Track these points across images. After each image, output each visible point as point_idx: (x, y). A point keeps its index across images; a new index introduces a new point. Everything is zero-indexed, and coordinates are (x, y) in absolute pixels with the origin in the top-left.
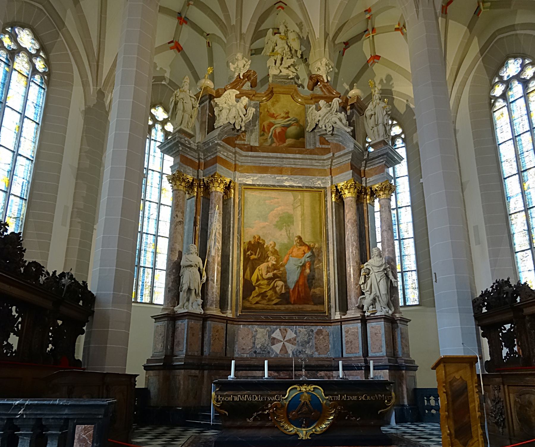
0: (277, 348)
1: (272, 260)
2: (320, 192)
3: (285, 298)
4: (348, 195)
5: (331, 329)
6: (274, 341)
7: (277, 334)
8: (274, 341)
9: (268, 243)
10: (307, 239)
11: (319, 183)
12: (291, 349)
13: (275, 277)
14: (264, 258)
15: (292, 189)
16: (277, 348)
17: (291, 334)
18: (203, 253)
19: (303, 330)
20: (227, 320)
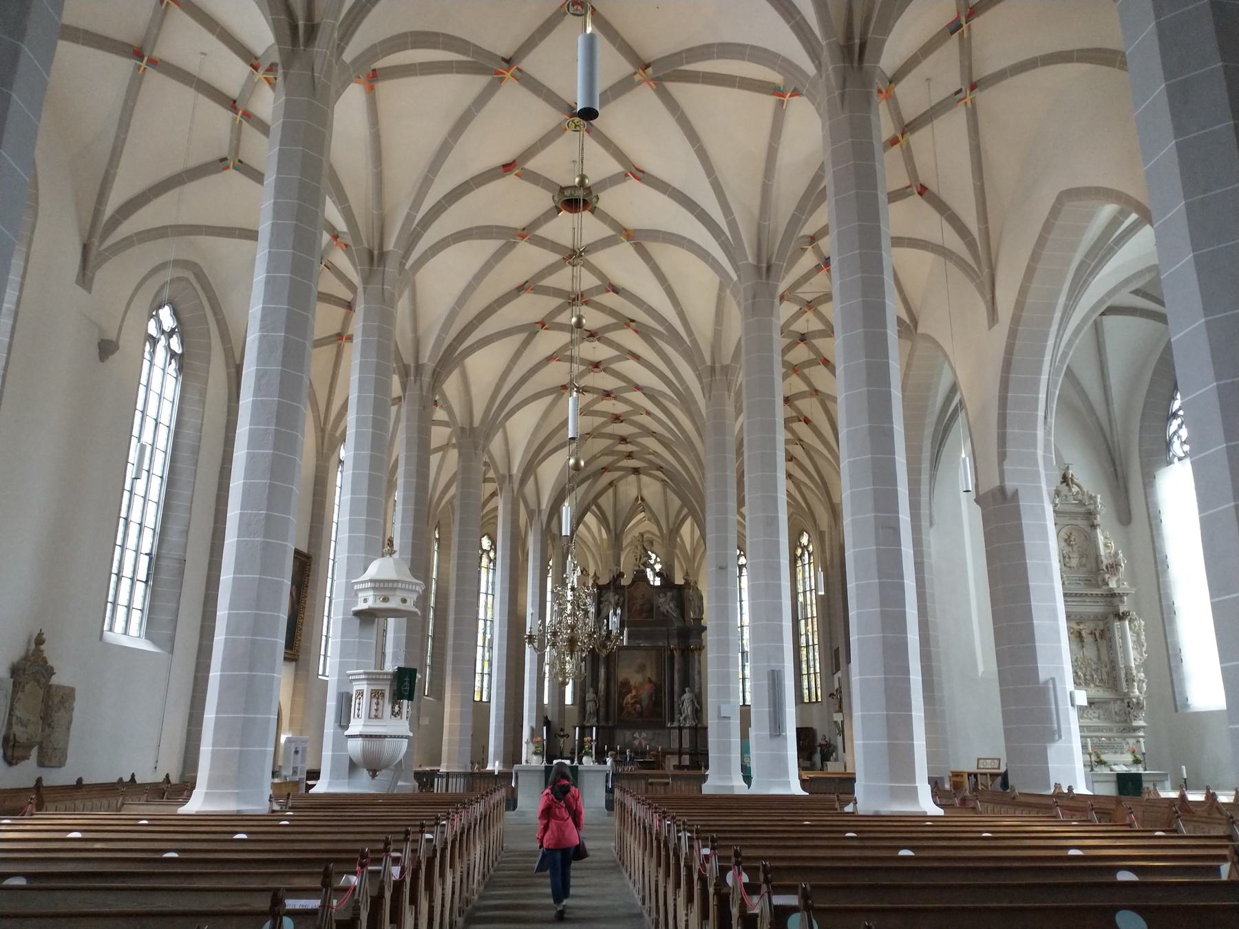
0: (636, 742)
1: (634, 692)
2: (659, 650)
3: (641, 714)
4: (676, 654)
5: (666, 731)
6: (635, 739)
7: (636, 735)
8: (635, 739)
9: (632, 682)
10: (654, 679)
11: (661, 644)
12: (644, 743)
13: (636, 702)
14: (630, 692)
15: (644, 648)
16: (636, 742)
17: (644, 735)
18: (596, 692)
19: (650, 733)
20: (610, 728)
